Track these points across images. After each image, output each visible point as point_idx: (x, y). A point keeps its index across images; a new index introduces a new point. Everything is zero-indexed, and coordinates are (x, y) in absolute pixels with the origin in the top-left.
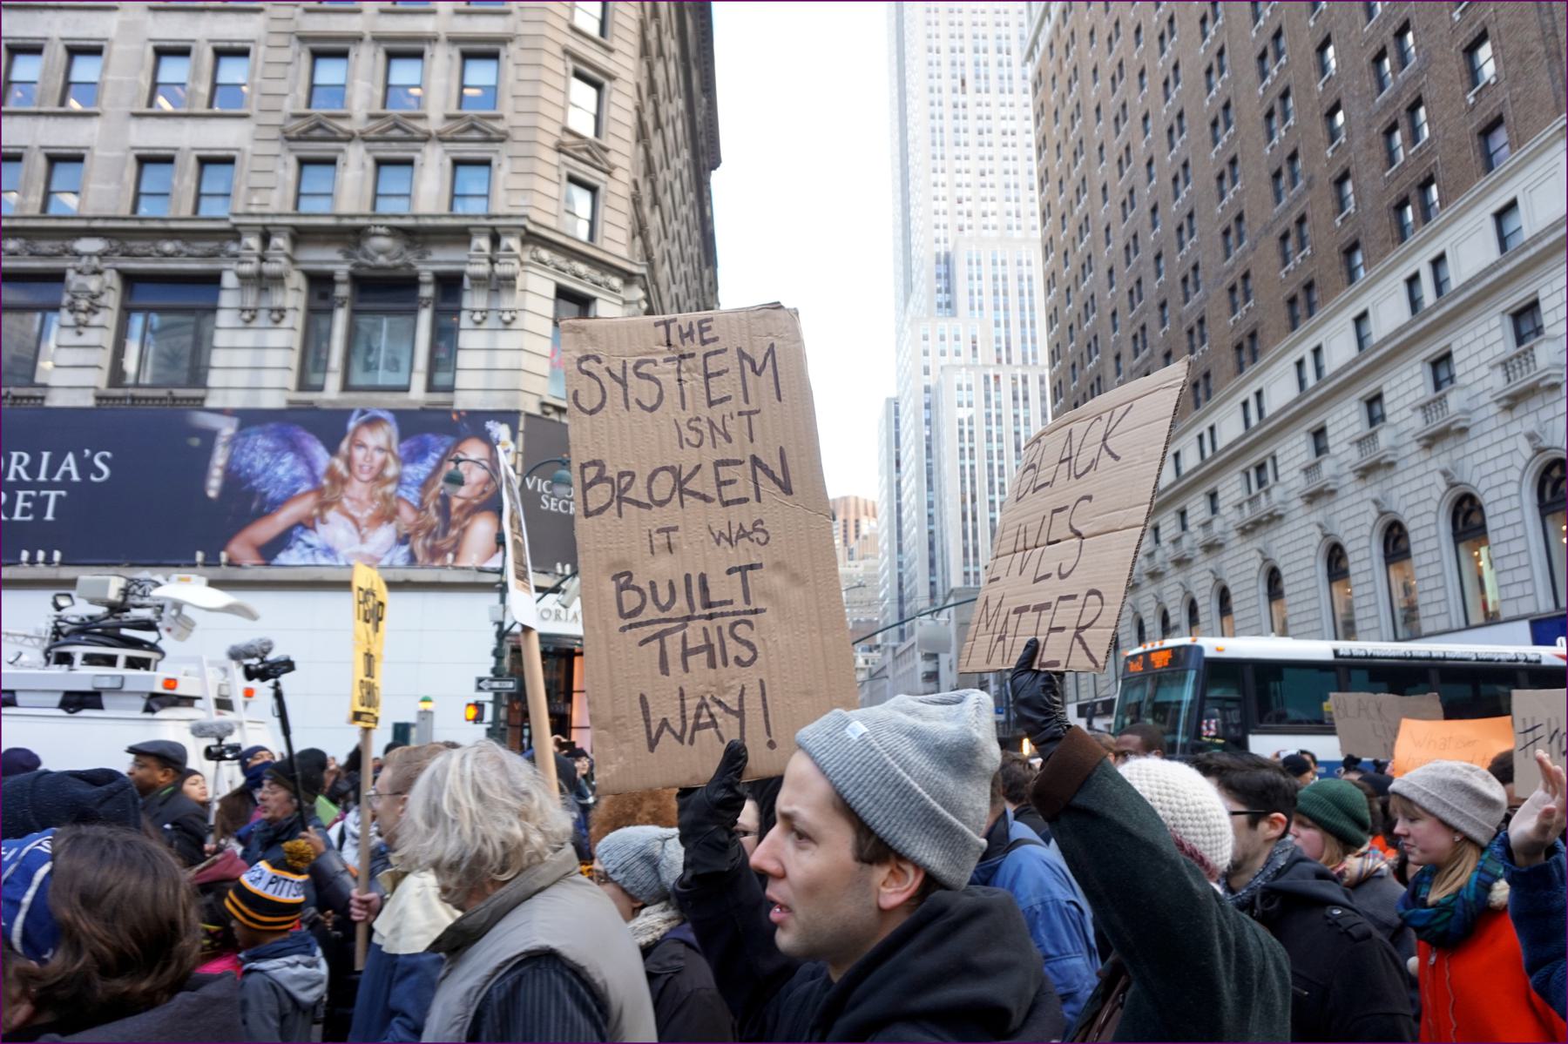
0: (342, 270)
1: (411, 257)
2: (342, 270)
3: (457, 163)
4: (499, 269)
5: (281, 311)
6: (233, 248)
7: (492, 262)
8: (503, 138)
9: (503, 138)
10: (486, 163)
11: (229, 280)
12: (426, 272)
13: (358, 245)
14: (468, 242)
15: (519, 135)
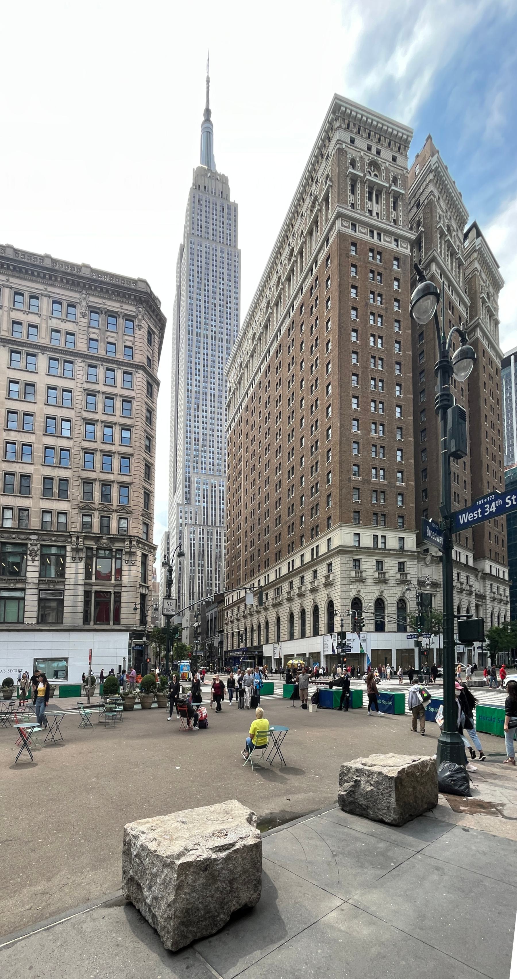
0: (95, 547)
1: (111, 545)
2: (95, 547)
3: (120, 518)
4: (132, 550)
5: (82, 558)
6: (69, 540)
7: (130, 548)
8: (131, 512)
9: (131, 512)
10: (127, 519)
11: (68, 548)
12: (114, 549)
13: (98, 541)
14: (125, 542)
15: (134, 512)
